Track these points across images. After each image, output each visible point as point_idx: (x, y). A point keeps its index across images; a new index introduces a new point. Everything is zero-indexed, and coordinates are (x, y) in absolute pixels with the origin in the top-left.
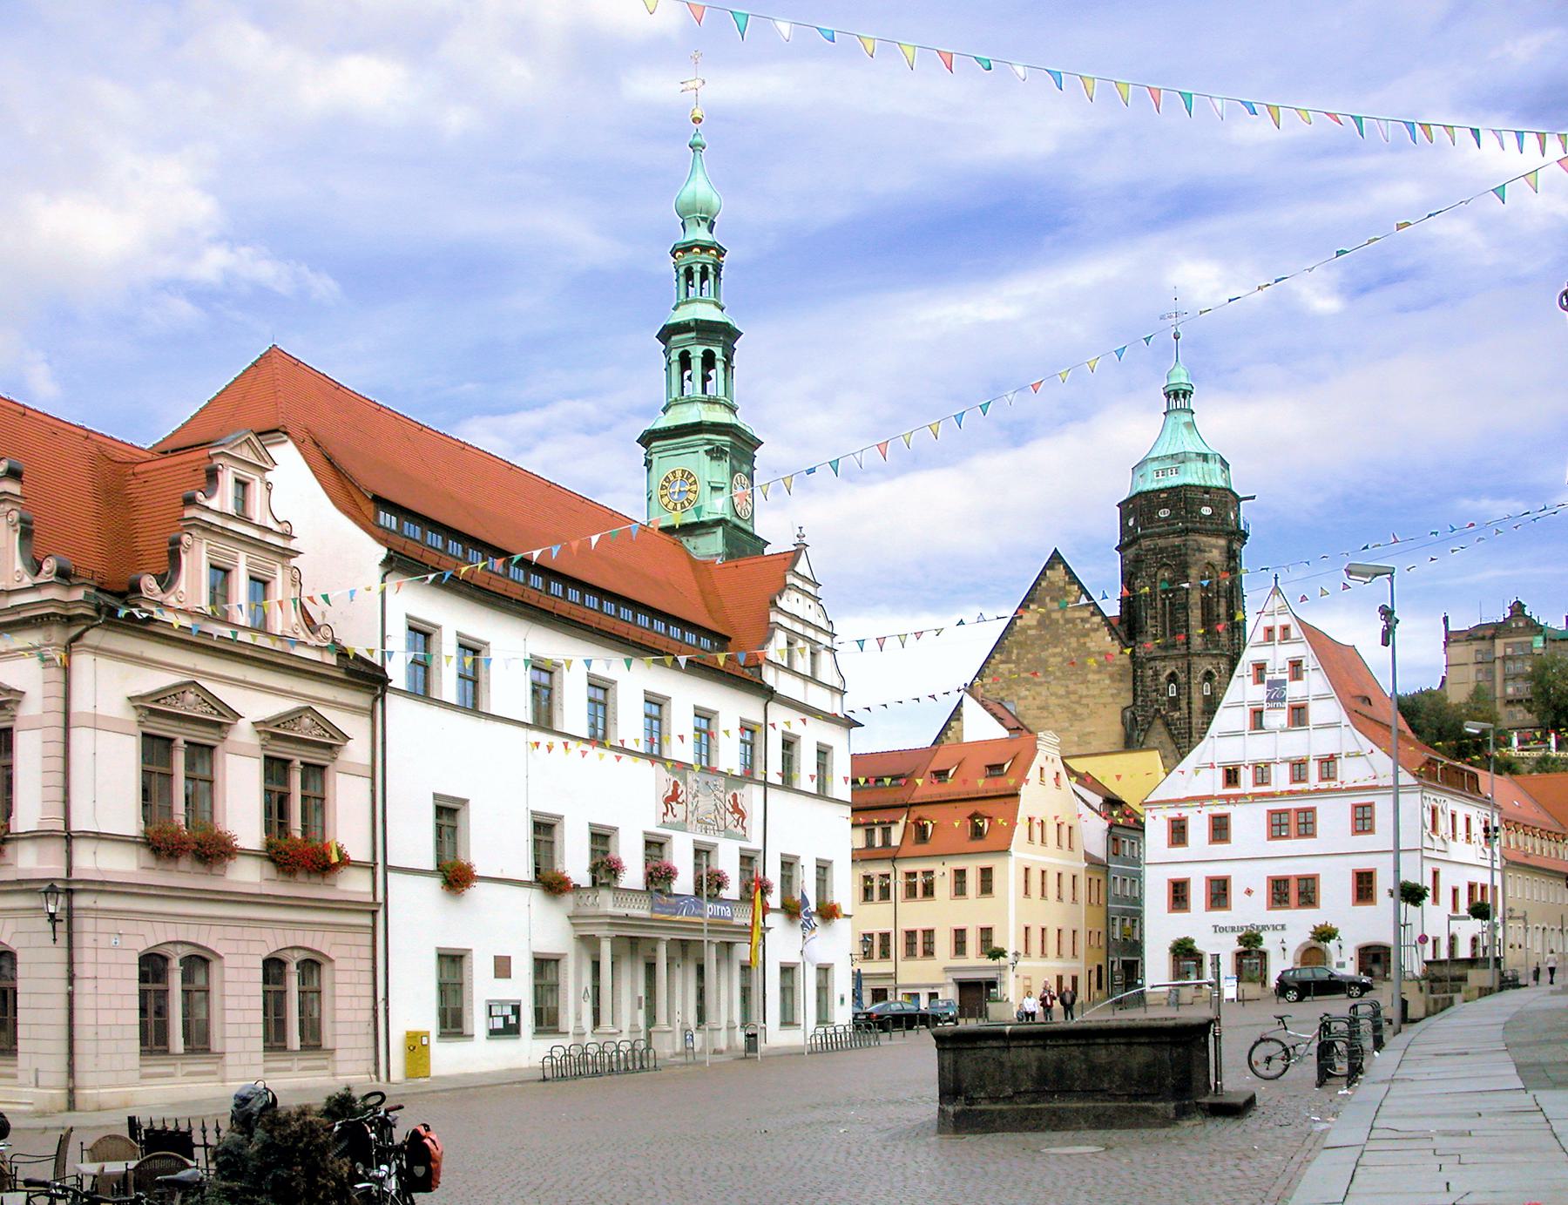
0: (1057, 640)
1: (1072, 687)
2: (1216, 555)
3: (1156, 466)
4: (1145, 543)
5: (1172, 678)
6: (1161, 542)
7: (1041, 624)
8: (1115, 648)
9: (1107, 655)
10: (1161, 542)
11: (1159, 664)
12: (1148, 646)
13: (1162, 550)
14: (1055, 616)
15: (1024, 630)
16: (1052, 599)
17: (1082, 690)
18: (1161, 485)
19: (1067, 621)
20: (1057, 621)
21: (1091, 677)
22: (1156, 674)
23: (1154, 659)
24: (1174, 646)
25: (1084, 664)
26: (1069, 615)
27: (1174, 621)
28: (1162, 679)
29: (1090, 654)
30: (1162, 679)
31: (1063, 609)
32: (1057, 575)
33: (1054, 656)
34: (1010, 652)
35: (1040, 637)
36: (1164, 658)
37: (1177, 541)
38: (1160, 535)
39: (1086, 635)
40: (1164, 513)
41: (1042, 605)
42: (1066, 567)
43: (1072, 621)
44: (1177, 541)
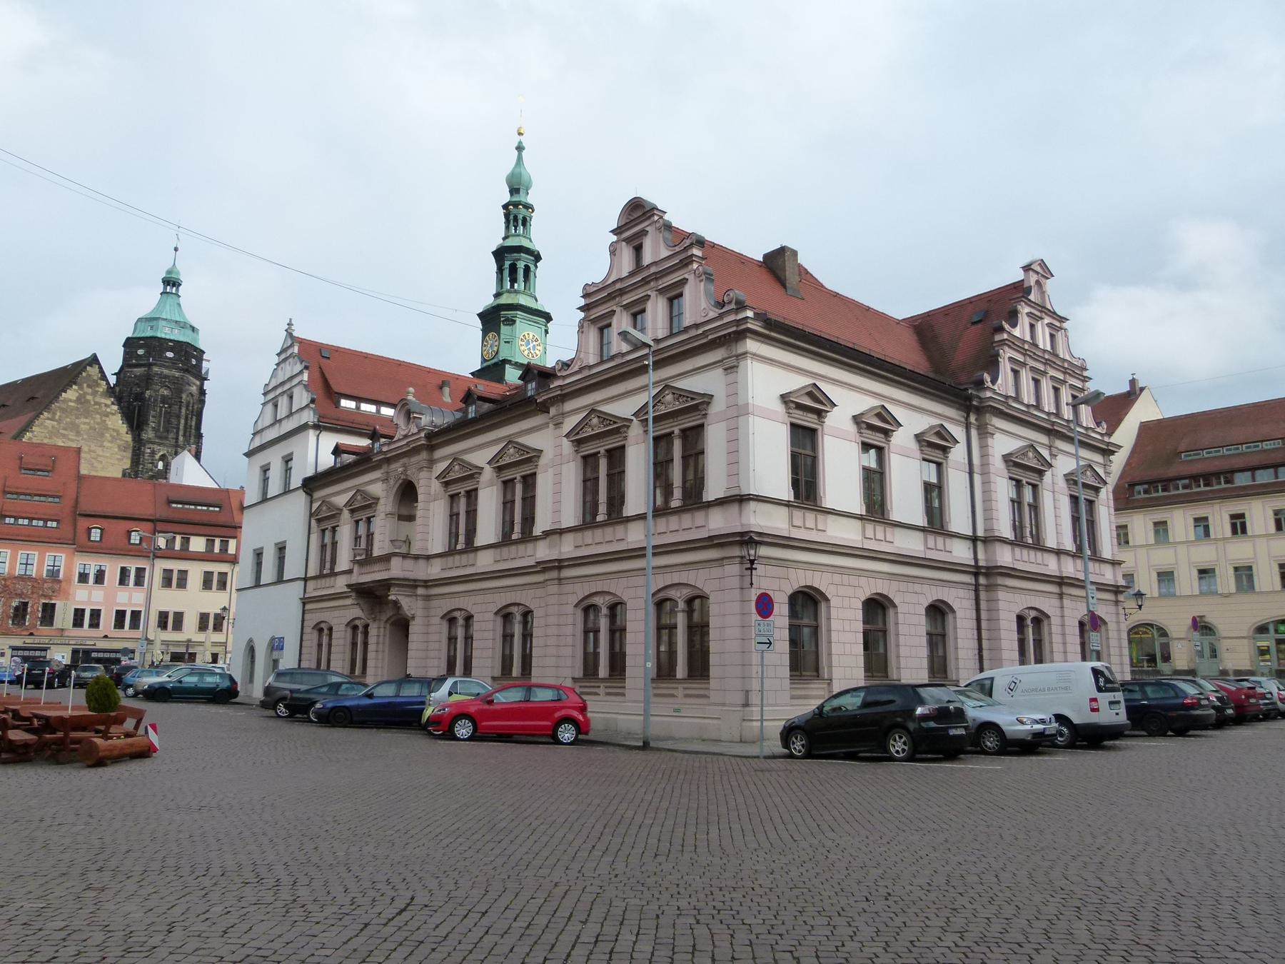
0: (87, 414)
1: (93, 447)
2: (194, 389)
3: (164, 323)
4: (156, 369)
5: (163, 458)
6: (166, 372)
7: (78, 400)
8: (123, 428)
9: (117, 432)
10: (166, 372)
11: (156, 447)
12: (148, 434)
13: (166, 377)
14: (89, 397)
15: (66, 401)
16: (89, 386)
17: (99, 451)
18: (172, 337)
19: (96, 403)
20: (88, 401)
21: (106, 444)
22: (153, 453)
23: (154, 443)
24: (166, 438)
25: (102, 435)
26: (98, 399)
27: (168, 422)
28: (157, 457)
29: (107, 429)
30: (157, 457)
31: (95, 393)
32: (93, 371)
33: (84, 423)
34: (54, 414)
35: (77, 409)
36: (160, 444)
37: (177, 374)
38: (166, 367)
39: (107, 415)
40: (170, 355)
41: (81, 388)
42: (101, 368)
43: (99, 404)
44: (177, 374)
